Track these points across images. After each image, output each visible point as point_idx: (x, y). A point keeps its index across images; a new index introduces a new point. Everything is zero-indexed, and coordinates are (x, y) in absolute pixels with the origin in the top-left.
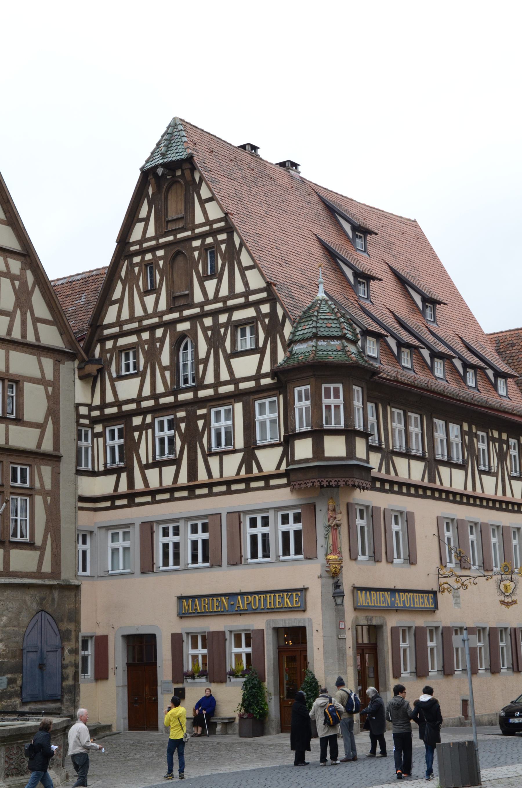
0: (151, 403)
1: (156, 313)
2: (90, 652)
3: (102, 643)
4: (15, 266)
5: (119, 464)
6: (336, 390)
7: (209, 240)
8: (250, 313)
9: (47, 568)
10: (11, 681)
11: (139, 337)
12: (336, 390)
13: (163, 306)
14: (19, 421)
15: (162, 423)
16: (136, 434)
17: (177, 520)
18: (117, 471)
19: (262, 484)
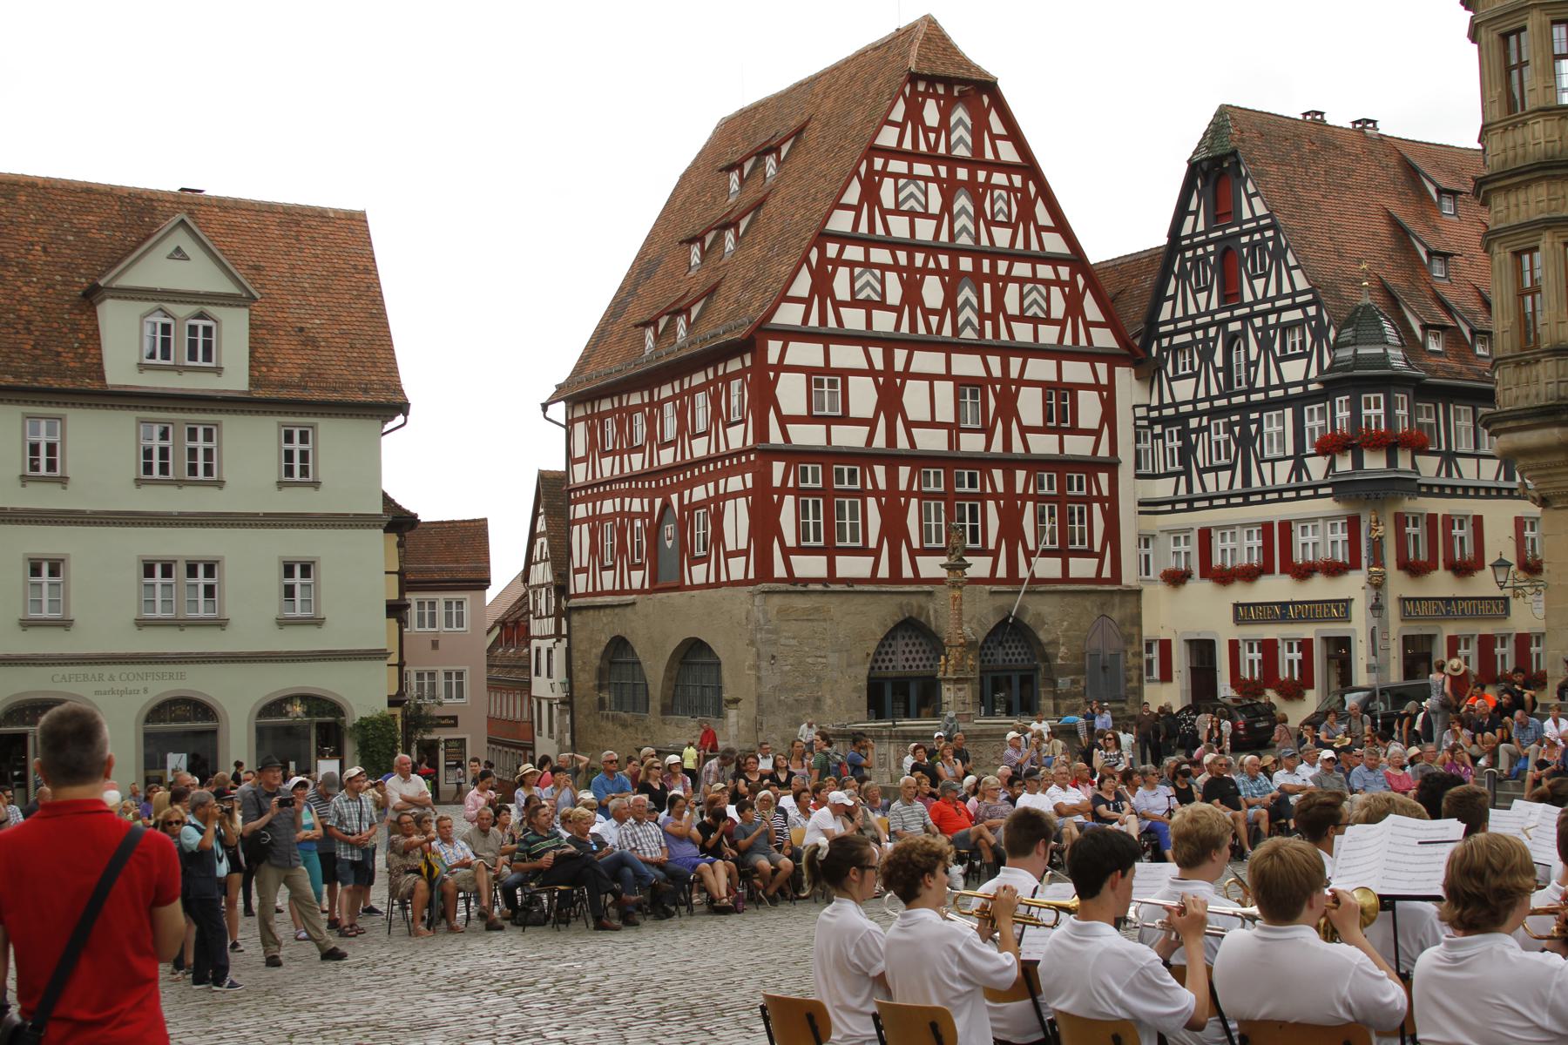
0: (1206, 405)
1: (1208, 312)
2: (1156, 653)
3: (1166, 646)
4: (1064, 273)
5: (1178, 467)
6: (1377, 400)
7: (1257, 237)
8: (1297, 314)
9: (1106, 573)
10: (1073, 682)
11: (1194, 336)
12: (1377, 400)
13: (1214, 305)
14: (1075, 430)
15: (1217, 425)
16: (1193, 436)
17: (1233, 526)
18: (1177, 474)
19: (1311, 492)
